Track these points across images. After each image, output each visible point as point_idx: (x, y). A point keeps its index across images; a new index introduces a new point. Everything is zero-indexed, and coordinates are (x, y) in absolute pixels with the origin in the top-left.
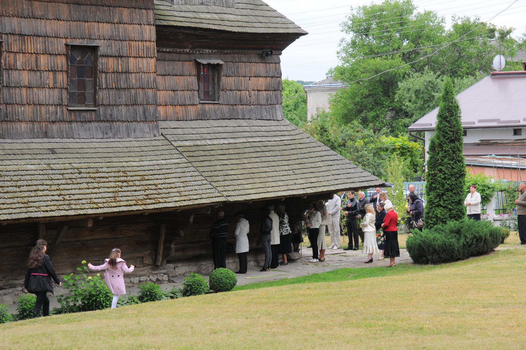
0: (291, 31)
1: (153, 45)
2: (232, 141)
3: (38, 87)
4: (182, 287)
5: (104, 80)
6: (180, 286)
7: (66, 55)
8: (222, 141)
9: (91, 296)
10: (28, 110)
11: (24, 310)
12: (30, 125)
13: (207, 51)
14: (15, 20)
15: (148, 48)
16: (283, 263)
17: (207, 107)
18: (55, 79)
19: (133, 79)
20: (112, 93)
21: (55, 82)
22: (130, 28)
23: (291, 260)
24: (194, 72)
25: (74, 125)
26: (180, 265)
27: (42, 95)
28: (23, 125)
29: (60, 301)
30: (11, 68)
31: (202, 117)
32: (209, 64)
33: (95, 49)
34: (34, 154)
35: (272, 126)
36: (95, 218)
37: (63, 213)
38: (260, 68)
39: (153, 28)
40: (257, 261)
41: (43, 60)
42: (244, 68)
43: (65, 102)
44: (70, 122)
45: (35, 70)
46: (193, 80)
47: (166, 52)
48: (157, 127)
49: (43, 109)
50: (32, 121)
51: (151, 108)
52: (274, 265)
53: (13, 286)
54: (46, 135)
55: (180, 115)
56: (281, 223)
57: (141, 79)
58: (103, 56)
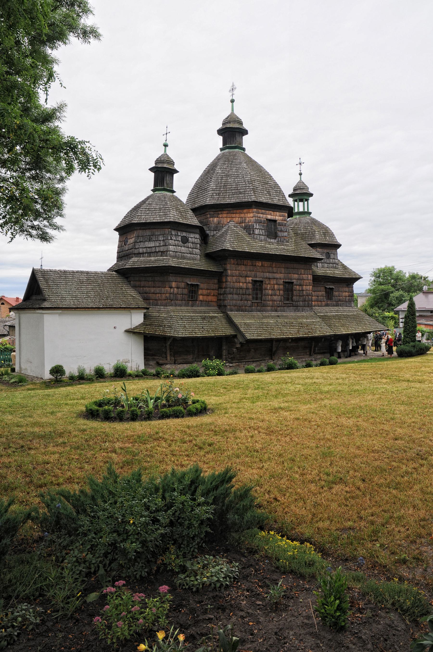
0: (357, 277)
1: (311, 281)
2: (337, 314)
3: (274, 295)
4: (319, 363)
6: (319, 362)
7: (283, 285)
8: (333, 314)
9: (290, 364)
10: (271, 303)
11: (269, 368)
12: (271, 308)
14: (267, 274)
15: (310, 282)
16: (353, 356)
17: (328, 302)
18: (279, 292)
19: (304, 293)
20: (298, 297)
21: (279, 294)
22: (304, 276)
23: (356, 355)
24: (324, 290)
25: (285, 308)
26: (318, 355)
27: (275, 298)
28: (269, 308)
29: (280, 365)
31: (327, 305)
32: (329, 288)
33: (293, 283)
34: (273, 317)
35: (351, 309)
36: (292, 339)
37: (281, 337)
38: (347, 289)
39: (311, 276)
40: (344, 355)
41: (276, 287)
42: (341, 289)
43: (283, 300)
44: (284, 307)
45: (273, 289)
46: (324, 293)
48: (312, 308)
49: (275, 302)
50: (272, 306)
51: (310, 302)
52: (350, 356)
53: (265, 360)
54: (276, 311)
55: (320, 305)
56: (353, 342)
57: (307, 293)
58: (295, 285)
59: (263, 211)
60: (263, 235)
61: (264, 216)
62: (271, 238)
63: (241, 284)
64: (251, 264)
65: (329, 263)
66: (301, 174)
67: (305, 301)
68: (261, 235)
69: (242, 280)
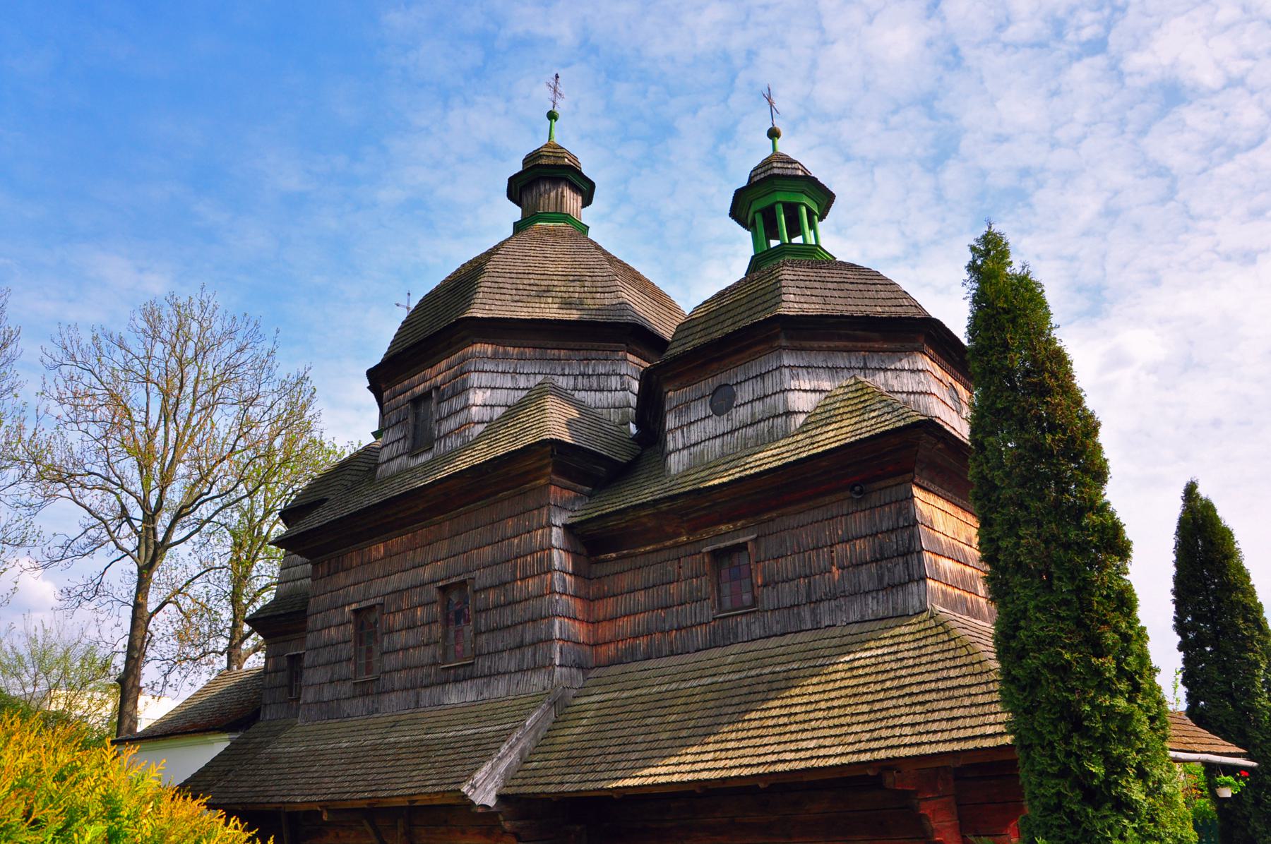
5: (483, 621)
10: (403, 674)
13: (724, 527)
15: (541, 561)
22: (516, 541)
30: (391, 631)
33: (464, 582)
45: (411, 627)
47: (649, 552)
59: (406, 382)
60: (397, 457)
61: (408, 394)
62: (417, 455)
63: (333, 630)
64: (359, 561)
65: (732, 432)
66: (773, 134)
67: (520, 646)
68: (392, 459)
69: (335, 617)
